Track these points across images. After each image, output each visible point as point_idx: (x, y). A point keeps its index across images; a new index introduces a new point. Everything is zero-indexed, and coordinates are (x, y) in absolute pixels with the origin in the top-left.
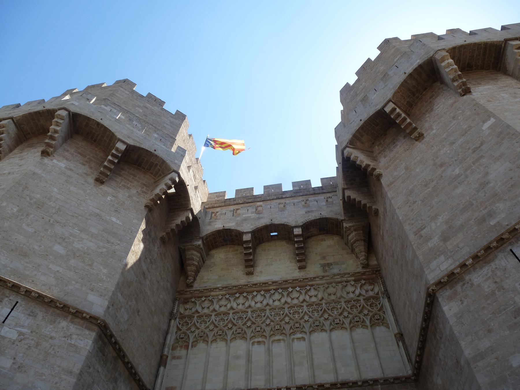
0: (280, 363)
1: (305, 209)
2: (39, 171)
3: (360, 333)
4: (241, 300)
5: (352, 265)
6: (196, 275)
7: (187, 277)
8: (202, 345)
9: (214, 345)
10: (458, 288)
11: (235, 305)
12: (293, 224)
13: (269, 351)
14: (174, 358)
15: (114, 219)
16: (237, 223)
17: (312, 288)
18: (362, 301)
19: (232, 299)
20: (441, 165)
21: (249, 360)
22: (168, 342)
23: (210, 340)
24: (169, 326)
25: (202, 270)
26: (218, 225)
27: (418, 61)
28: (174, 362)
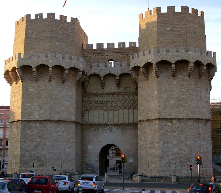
0: (111, 117)
1: (121, 68)
2: (51, 88)
3: (131, 111)
4: (101, 98)
5: (132, 89)
6: (87, 87)
7: (84, 89)
8: (92, 111)
9: (95, 111)
10: (141, 123)
11: (99, 99)
12: (116, 74)
13: (108, 114)
14: (85, 114)
15: (70, 93)
16: (99, 71)
17: (121, 95)
18: (133, 102)
19: (98, 97)
20: (147, 94)
21: (104, 116)
22: (83, 110)
23: (94, 109)
24: (82, 105)
25: (89, 85)
26: (93, 71)
27: (150, 60)
28: (85, 115)
